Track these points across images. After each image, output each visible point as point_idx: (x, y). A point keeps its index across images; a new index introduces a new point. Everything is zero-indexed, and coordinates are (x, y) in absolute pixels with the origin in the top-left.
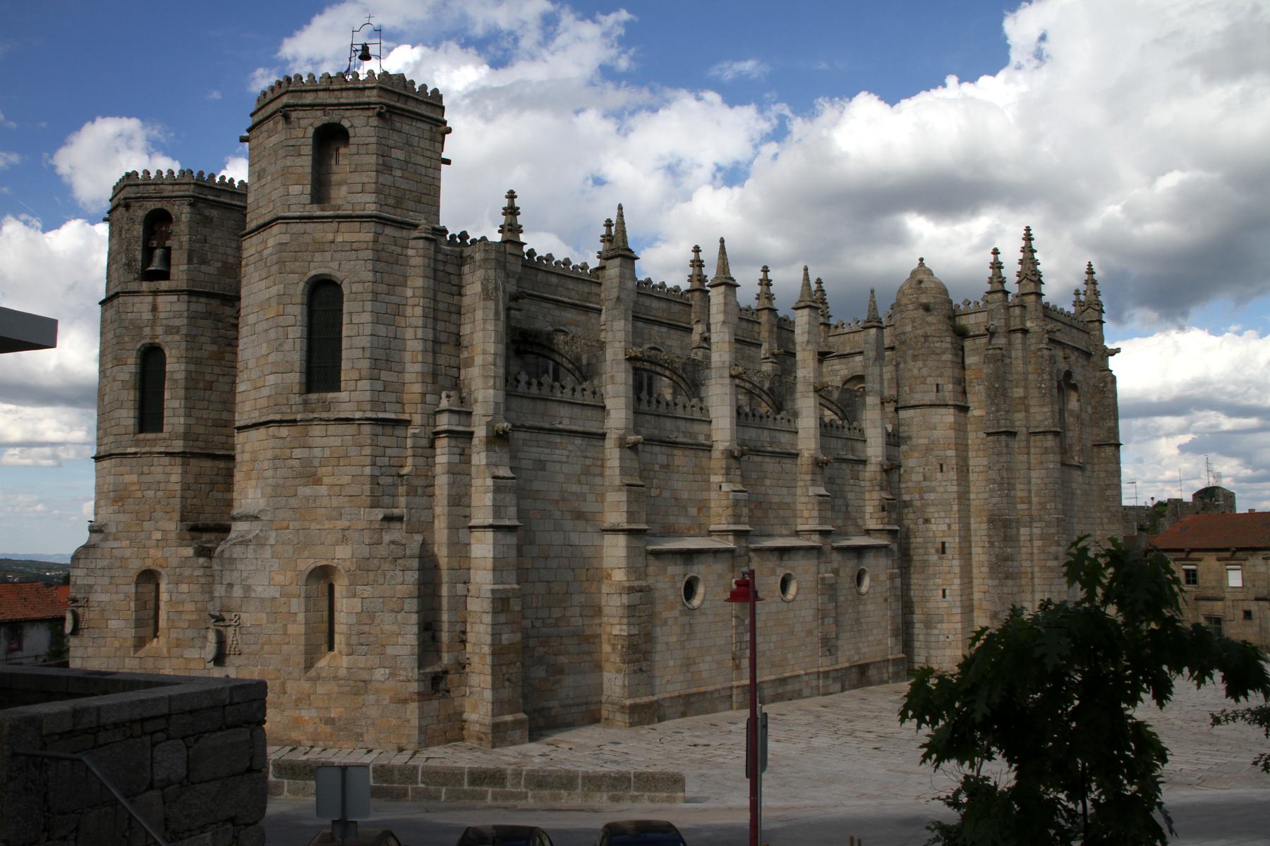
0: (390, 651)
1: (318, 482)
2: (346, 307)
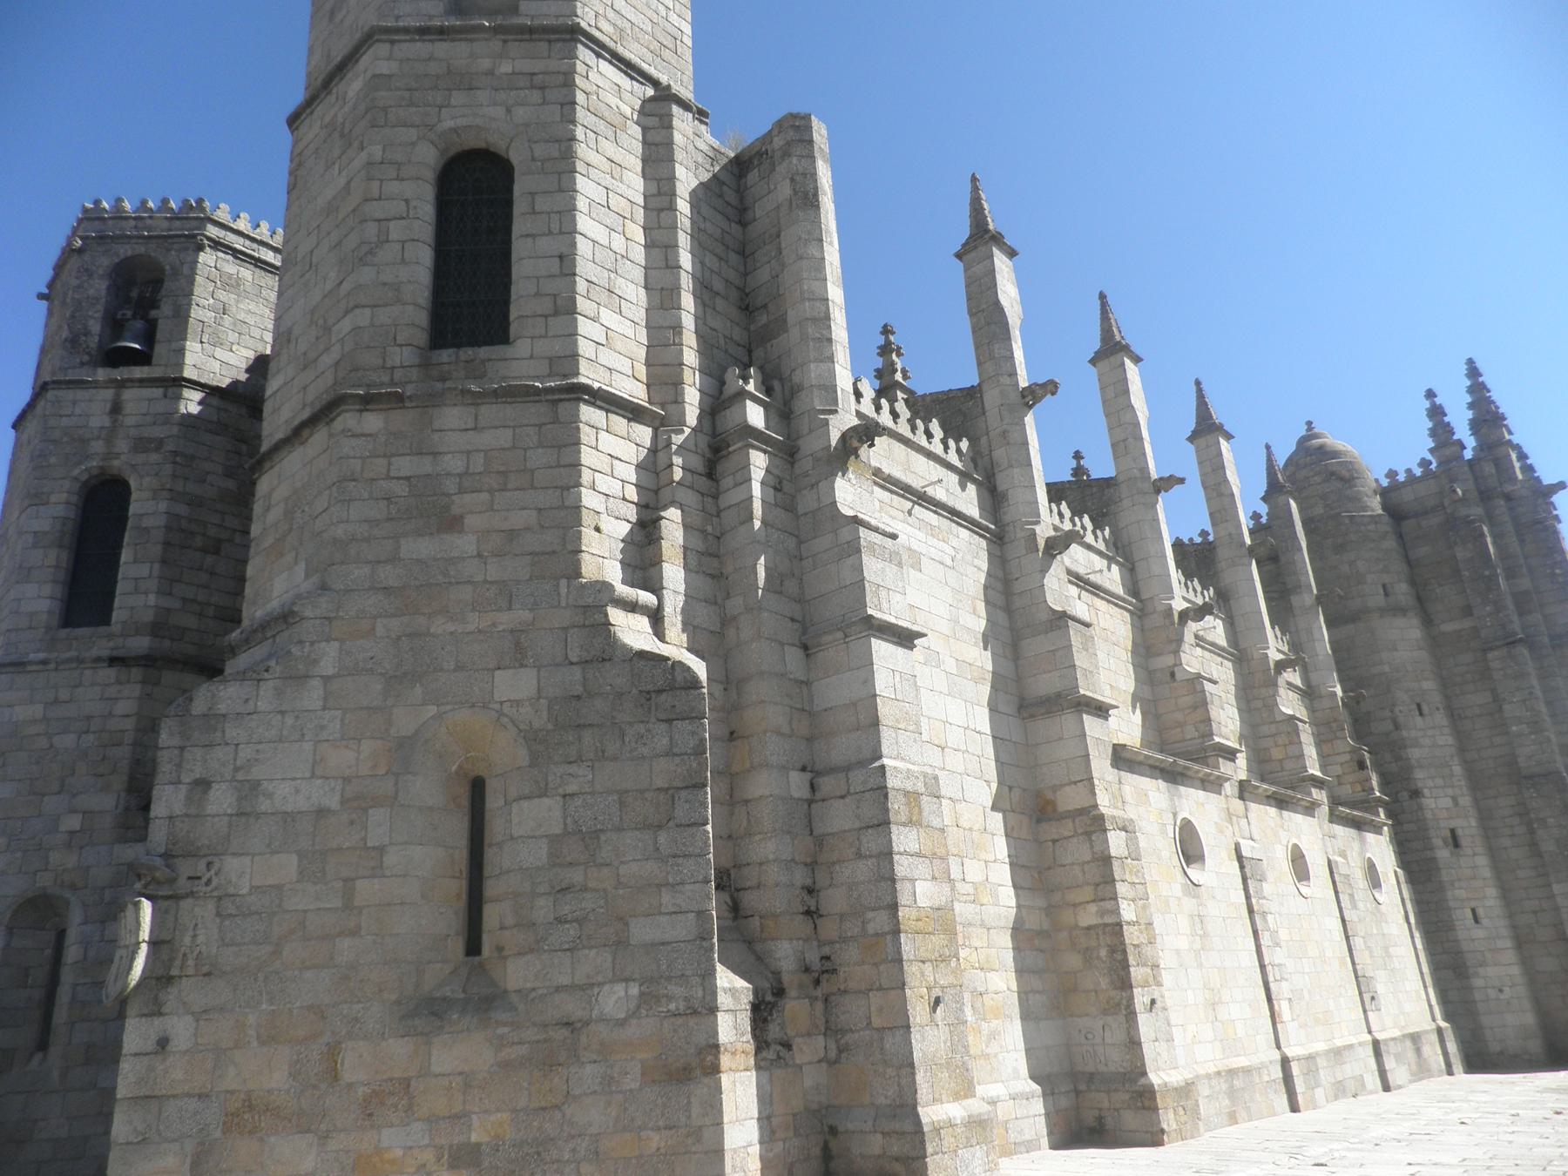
0: (642, 931)
1: (452, 524)
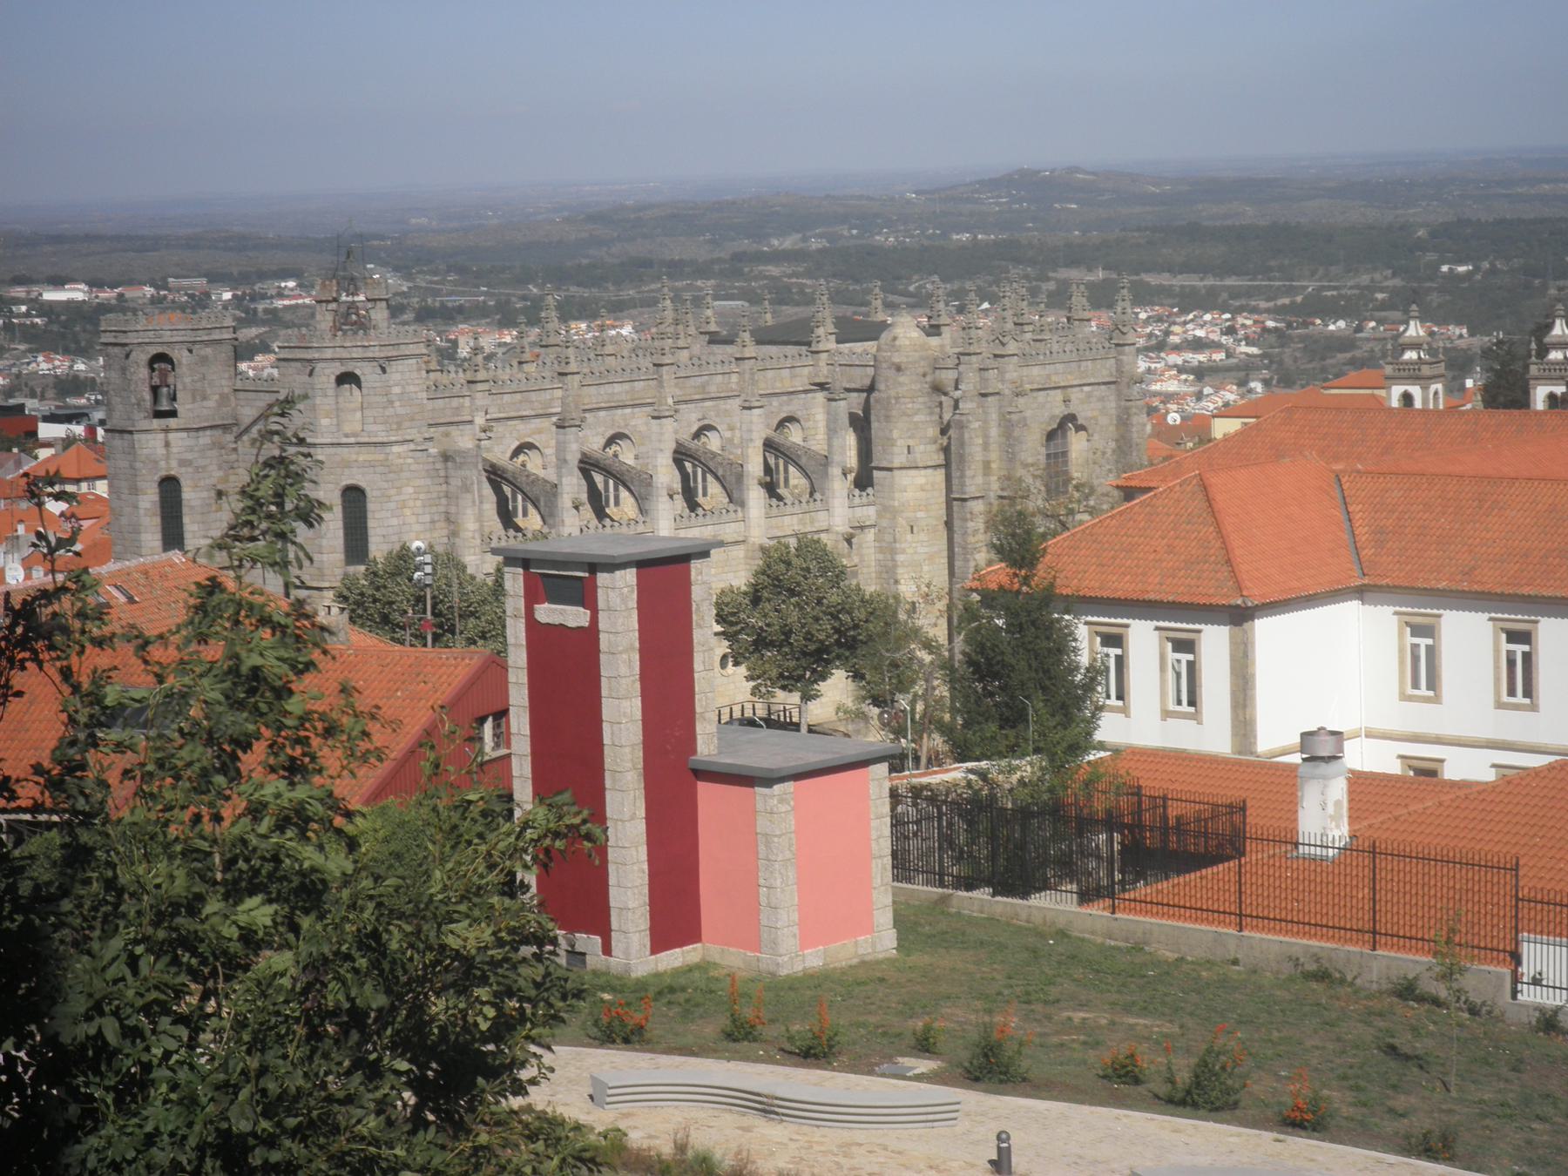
2: (370, 506)
